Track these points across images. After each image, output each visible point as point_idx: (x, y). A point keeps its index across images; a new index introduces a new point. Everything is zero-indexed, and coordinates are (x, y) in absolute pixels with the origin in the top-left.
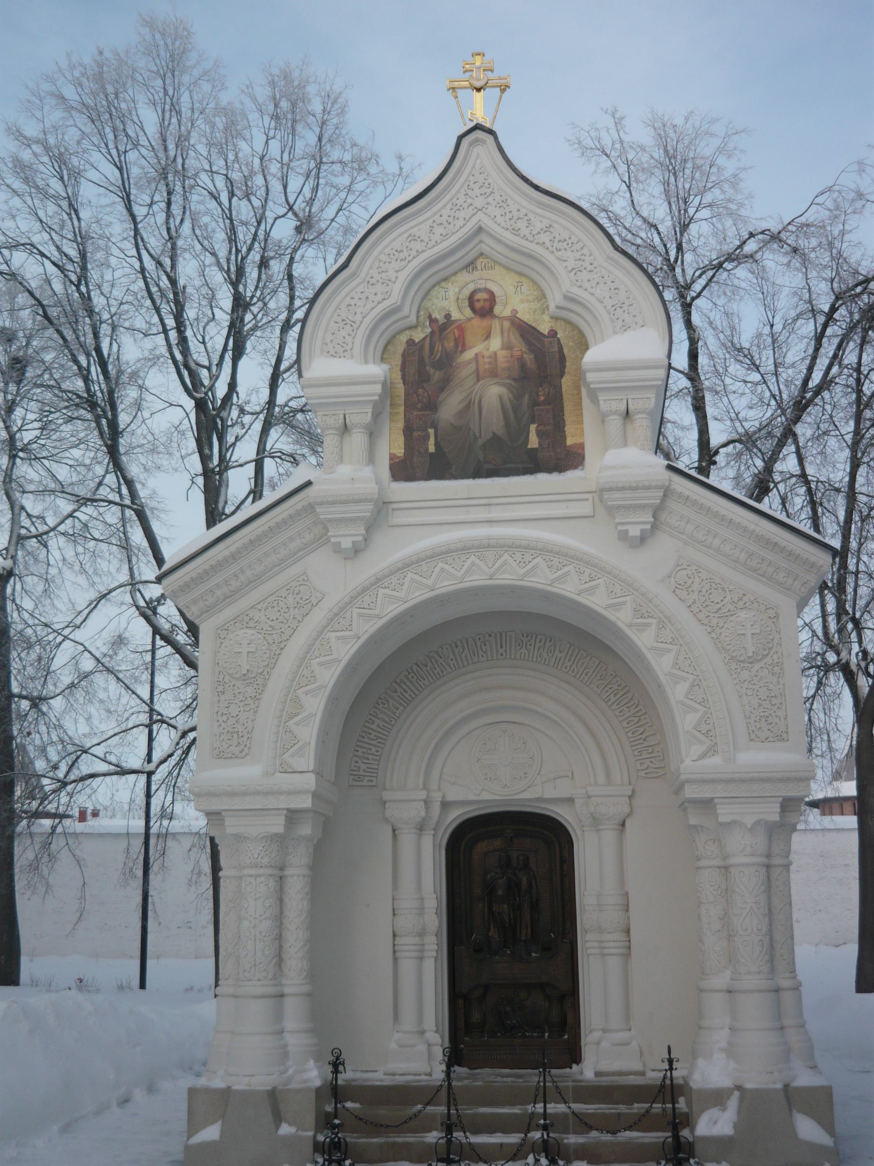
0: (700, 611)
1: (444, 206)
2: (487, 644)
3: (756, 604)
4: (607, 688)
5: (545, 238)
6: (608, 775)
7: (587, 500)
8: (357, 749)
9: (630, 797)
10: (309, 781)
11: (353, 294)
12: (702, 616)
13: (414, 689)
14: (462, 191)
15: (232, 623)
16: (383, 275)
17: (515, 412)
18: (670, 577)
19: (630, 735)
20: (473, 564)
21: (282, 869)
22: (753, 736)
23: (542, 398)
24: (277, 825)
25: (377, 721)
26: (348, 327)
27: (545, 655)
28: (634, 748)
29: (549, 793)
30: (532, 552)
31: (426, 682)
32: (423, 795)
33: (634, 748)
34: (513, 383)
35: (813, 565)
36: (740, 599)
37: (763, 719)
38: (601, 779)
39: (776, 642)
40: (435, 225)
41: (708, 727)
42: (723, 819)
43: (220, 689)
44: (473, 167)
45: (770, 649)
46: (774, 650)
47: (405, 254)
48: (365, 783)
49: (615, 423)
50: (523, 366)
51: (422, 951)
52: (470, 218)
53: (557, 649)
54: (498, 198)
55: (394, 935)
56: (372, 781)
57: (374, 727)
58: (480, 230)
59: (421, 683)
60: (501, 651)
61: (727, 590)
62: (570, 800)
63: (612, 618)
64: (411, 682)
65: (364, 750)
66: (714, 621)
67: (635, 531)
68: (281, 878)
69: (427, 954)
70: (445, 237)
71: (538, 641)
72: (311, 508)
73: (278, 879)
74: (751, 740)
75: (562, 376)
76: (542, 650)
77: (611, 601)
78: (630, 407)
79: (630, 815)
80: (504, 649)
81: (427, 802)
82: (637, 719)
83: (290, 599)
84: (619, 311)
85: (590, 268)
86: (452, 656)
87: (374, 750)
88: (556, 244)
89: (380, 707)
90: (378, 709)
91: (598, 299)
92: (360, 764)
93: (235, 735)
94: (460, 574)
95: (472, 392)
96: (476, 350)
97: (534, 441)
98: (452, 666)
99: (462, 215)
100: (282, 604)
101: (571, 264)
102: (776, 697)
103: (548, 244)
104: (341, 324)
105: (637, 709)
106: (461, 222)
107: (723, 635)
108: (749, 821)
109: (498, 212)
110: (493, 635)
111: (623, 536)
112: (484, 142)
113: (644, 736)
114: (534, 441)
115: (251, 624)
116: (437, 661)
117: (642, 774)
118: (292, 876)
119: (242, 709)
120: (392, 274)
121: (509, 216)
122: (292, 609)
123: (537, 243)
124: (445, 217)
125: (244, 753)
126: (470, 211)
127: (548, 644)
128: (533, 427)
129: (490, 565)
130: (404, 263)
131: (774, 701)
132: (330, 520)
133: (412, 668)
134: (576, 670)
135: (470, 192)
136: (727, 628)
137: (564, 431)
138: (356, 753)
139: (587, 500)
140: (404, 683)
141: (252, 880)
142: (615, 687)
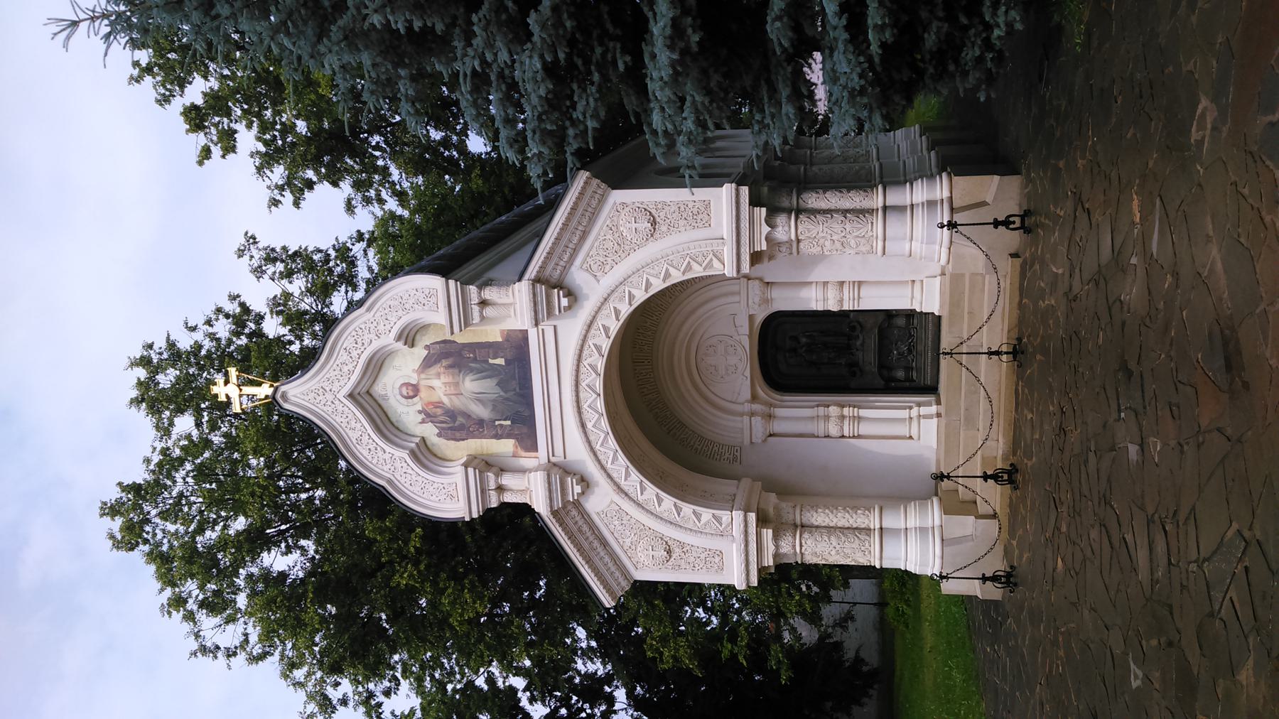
1: (335, 421)
3: (615, 218)
5: (354, 354)
6: (733, 294)
7: (543, 330)
9: (749, 279)
10: (738, 515)
11: (403, 482)
12: (623, 256)
14: (323, 407)
17: (482, 372)
20: (589, 406)
21: (795, 526)
22: (707, 225)
23: (471, 355)
24: (768, 534)
25: (696, 446)
27: (649, 333)
29: (745, 329)
30: (581, 368)
32: (746, 419)
35: (586, 183)
38: (736, 298)
41: (701, 255)
42: (764, 247)
43: (677, 568)
45: (645, 210)
46: (646, 207)
47: (371, 447)
48: (738, 454)
49: (488, 311)
50: (450, 366)
51: (854, 417)
54: (326, 384)
55: (843, 436)
57: (700, 448)
58: (351, 396)
62: (751, 318)
63: (626, 315)
66: (627, 247)
67: (565, 302)
68: (803, 526)
69: (856, 415)
70: (357, 420)
72: (555, 513)
73: (803, 529)
77: (614, 316)
79: (761, 279)
81: (752, 414)
85: (375, 324)
87: (716, 448)
92: (726, 457)
94: (597, 416)
97: (500, 361)
99: (340, 408)
100: (620, 528)
101: (373, 336)
104: (425, 490)
108: (766, 229)
109: (336, 384)
111: (569, 307)
112: (284, 392)
114: (500, 361)
115: (634, 548)
118: (801, 519)
120: (387, 456)
121: (339, 377)
124: (342, 420)
126: (337, 402)
128: (491, 361)
130: (379, 448)
132: (562, 500)
135: (322, 403)
139: (543, 330)
141: (803, 549)
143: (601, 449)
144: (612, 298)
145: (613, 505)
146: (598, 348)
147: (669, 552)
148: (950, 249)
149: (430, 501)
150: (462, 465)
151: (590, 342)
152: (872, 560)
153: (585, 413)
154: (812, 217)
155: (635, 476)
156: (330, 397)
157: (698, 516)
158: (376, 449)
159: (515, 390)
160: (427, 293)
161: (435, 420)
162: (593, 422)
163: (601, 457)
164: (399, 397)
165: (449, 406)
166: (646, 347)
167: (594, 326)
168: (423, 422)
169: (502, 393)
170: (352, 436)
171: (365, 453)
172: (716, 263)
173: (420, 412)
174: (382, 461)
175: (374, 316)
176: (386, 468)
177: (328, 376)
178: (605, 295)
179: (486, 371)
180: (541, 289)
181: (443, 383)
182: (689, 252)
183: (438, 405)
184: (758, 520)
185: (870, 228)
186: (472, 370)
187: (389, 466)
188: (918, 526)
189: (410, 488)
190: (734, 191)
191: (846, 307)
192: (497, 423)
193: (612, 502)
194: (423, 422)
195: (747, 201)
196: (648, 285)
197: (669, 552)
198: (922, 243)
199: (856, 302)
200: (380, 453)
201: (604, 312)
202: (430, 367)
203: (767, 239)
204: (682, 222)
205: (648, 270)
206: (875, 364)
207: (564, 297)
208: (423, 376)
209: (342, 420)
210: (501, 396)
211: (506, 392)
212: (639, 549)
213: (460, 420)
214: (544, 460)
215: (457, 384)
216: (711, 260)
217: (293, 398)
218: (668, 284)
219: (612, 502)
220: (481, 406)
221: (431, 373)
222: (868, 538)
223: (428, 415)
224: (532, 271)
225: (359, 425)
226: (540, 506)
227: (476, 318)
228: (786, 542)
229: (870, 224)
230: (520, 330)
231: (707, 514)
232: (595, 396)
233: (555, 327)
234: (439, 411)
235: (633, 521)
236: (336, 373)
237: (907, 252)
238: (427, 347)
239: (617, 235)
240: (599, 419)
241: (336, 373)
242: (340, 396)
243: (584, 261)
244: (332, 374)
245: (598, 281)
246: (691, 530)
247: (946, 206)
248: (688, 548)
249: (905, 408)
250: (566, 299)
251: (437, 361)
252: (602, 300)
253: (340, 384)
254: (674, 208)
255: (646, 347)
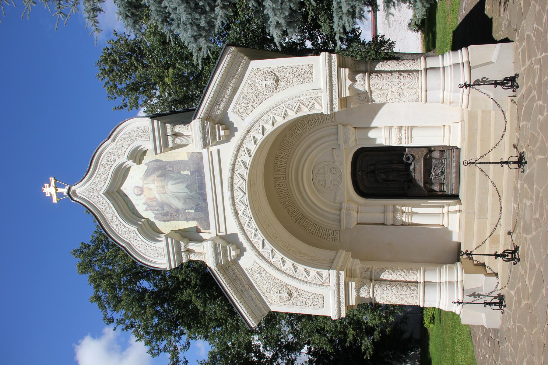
0: (256, 103)
2: (279, 184)
3: (253, 79)
4: (297, 134)
5: (107, 168)
8: (324, 238)
10: (333, 273)
13: (298, 215)
15: (268, 298)
16: (127, 233)
17: (177, 179)
18: (242, 117)
19: (316, 125)
20: (240, 201)
23: (171, 169)
25: (312, 230)
26: (148, 248)
27: (284, 160)
28: (322, 123)
31: (296, 209)
33: (322, 123)
34: (166, 179)
36: (251, 86)
37: (303, 76)
39: (269, 70)
40: (106, 211)
41: (307, 101)
43: (295, 304)
44: (83, 195)
45: (272, 72)
47: (117, 223)
48: (338, 235)
49: (179, 141)
52: (102, 197)
53: (281, 155)
56: (337, 233)
57: (315, 231)
59: (296, 211)
60: (282, 178)
61: (247, 91)
63: (261, 141)
64: (296, 215)
65: (324, 235)
66: (261, 97)
71: (277, 163)
74: (312, 81)
75: (163, 161)
76: (281, 161)
78: (170, 134)
80: (281, 177)
82: (310, 122)
83: (258, 275)
84: (133, 138)
86: (285, 199)
87: (324, 231)
88: (109, 163)
89: (306, 228)
90: (307, 229)
91: (129, 147)
93: (314, 300)
94: (244, 207)
95: (171, 196)
96: (155, 193)
98: (289, 198)
101: (116, 157)
102: (293, 70)
103: (109, 166)
105: (305, 122)
106: (104, 201)
107: (266, 93)
108: (349, 82)
109: (99, 186)
110: (275, 181)
113: (317, 119)
116: (287, 205)
117: (333, 120)
119: (303, 297)
120: (126, 229)
122: (262, 275)
123: (110, 170)
124: (102, 207)
125: (322, 297)
127: (279, 159)
128: (182, 172)
129: (240, 194)
131: (295, 71)
133: (290, 215)
134: (289, 147)
135: (93, 197)
136: (263, 92)
137: (183, 160)
138: (326, 239)
139: (211, 152)
140: (296, 218)
142: (296, 131)
143: (247, 228)
144: (252, 130)
145: (255, 264)
146: (244, 163)
147: (290, 294)
148: (468, 95)
149: (149, 257)
150: (164, 236)
151: (239, 159)
152: (418, 302)
153: (237, 205)
154: (379, 75)
155: (268, 246)
156: (96, 194)
157: (308, 273)
158: (121, 225)
159: (196, 191)
160: (143, 129)
161: (152, 208)
162: (242, 210)
163: (248, 234)
164: (134, 195)
165: (160, 201)
166: (281, 169)
167: (241, 149)
168: (146, 210)
169: (189, 193)
170: (108, 217)
171: (115, 227)
172: (317, 106)
173: (144, 204)
174: (124, 232)
175: (116, 145)
176: (125, 236)
177: (94, 181)
178: (248, 129)
179: (179, 179)
180: (208, 124)
181: (156, 186)
182: (299, 99)
183: (154, 199)
184: (346, 275)
185: (417, 82)
186: (171, 178)
187: (127, 235)
188: (447, 281)
189: (138, 249)
190: (327, 57)
191: (403, 145)
192: (187, 211)
193: (255, 262)
194: (146, 210)
195: (336, 64)
196: (274, 122)
197: (290, 294)
198: (451, 92)
199: (409, 139)
200: (123, 228)
201: (247, 140)
202: (149, 176)
203: (349, 89)
204: (295, 79)
205: (274, 112)
206: (421, 181)
207: (222, 130)
208: (145, 182)
209: (102, 207)
210: (188, 194)
211: (191, 191)
212: (272, 292)
213: (166, 209)
214: (214, 235)
215: (163, 187)
216: (314, 104)
217: (78, 194)
218: (286, 120)
219: (255, 262)
220: (177, 201)
221: (150, 180)
222: (416, 288)
223: (149, 206)
224: (202, 112)
225: (111, 210)
226: (211, 263)
227: (170, 145)
228: (364, 290)
229: (417, 79)
230: (198, 153)
231: (313, 271)
232: (243, 194)
233: (218, 150)
234: (155, 203)
235: (268, 274)
236: (99, 179)
237: (441, 100)
238: (147, 164)
239: (254, 90)
240: (245, 209)
241: (99, 179)
242: (101, 193)
243: (234, 108)
244: (96, 180)
245: (244, 120)
246: (304, 281)
247: (466, 66)
248: (302, 292)
249: (440, 207)
250: (223, 131)
251: (152, 173)
252: (245, 131)
253: (100, 186)
254: (289, 70)
255: (281, 169)
